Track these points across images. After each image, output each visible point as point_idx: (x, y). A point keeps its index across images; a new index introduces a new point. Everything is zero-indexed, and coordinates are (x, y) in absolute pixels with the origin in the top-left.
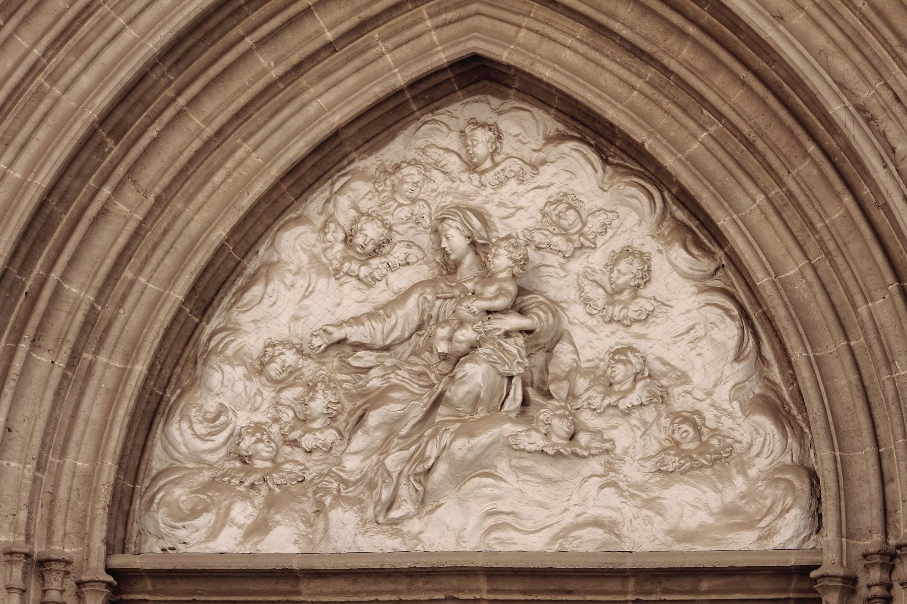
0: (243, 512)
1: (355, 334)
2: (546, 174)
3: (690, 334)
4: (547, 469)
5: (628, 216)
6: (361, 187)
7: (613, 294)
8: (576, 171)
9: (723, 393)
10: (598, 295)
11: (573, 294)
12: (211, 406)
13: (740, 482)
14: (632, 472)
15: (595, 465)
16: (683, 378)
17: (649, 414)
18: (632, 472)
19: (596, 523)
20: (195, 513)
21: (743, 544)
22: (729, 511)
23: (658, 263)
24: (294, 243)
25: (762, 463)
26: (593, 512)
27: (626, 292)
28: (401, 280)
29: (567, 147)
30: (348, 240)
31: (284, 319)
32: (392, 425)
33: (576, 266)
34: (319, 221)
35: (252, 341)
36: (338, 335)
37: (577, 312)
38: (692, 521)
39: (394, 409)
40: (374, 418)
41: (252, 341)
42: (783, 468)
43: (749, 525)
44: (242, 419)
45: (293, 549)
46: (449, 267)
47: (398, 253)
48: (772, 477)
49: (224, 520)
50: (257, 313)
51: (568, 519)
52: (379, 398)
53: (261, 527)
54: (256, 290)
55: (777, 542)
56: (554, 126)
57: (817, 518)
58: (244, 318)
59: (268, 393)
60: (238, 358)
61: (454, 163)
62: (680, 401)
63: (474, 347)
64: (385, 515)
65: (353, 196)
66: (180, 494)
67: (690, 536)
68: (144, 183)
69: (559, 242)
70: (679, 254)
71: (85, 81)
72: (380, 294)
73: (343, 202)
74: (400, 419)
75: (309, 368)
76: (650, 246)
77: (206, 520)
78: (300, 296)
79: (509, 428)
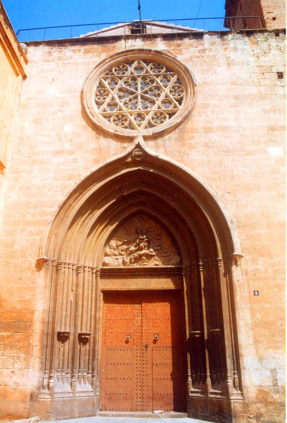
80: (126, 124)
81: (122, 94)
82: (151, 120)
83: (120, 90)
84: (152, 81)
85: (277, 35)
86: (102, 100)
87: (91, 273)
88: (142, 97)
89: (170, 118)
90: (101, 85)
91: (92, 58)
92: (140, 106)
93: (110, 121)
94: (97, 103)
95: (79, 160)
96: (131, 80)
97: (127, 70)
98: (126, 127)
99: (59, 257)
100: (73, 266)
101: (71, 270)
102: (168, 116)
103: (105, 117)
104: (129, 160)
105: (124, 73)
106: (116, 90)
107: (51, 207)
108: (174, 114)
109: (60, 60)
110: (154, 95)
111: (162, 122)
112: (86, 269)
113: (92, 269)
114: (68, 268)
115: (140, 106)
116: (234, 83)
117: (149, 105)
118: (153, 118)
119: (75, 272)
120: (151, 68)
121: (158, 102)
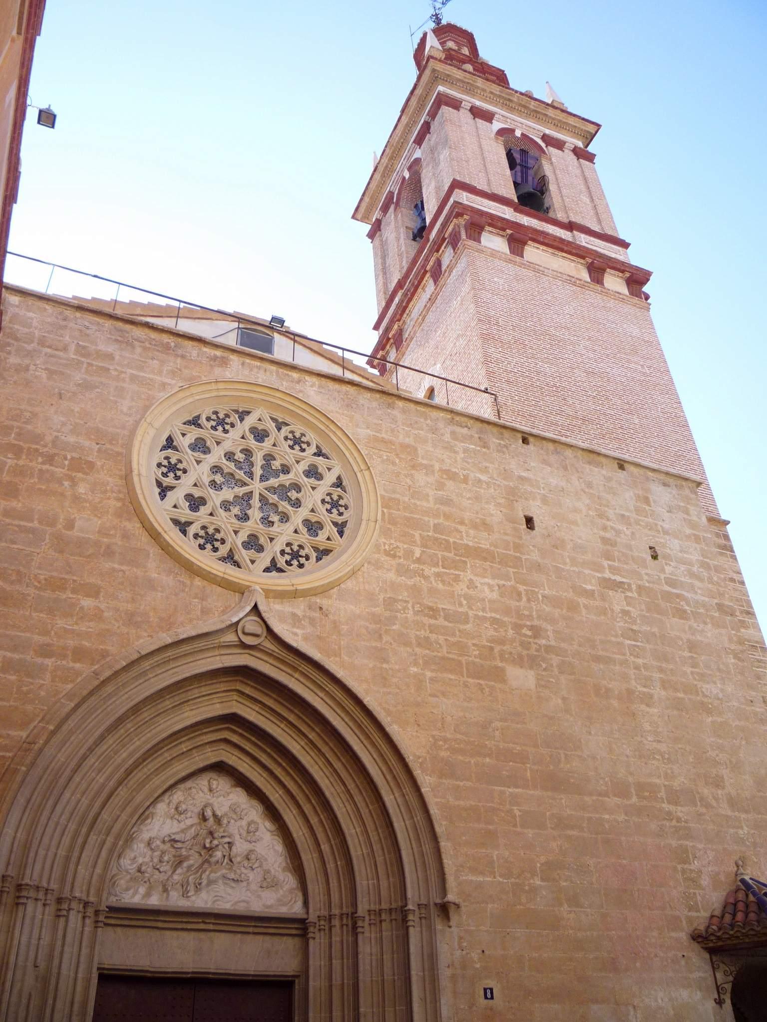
0: (142, 890)
1: (177, 837)
2: (231, 796)
3: (269, 847)
4: (233, 885)
5: (253, 812)
6: (180, 793)
7: (248, 832)
8: (239, 797)
9: (276, 865)
10: (244, 834)
11: (236, 832)
12: (132, 855)
13: (281, 891)
14: (253, 887)
15: (245, 884)
16: (266, 860)
17: (259, 869)
18: (253, 887)
19: (244, 901)
20: (128, 889)
21: (283, 911)
22: (279, 900)
23: (261, 827)
24: (161, 807)
25: (286, 887)
26: (243, 898)
27: (251, 831)
28: (189, 822)
29: (239, 789)
30: (177, 808)
31: (156, 831)
32: (189, 867)
33: (239, 823)
34: (167, 801)
35: (146, 836)
36: (173, 837)
37: (237, 837)
38: (269, 903)
39: (191, 862)
40: (185, 864)
41: (146, 836)
42: (294, 889)
43: (284, 905)
44: (140, 860)
45: (156, 903)
46: (204, 819)
47: (189, 815)
48: (291, 891)
49: (136, 892)
50: (149, 827)
51: (236, 899)
52: (187, 858)
53: (148, 895)
54: (149, 821)
55: (293, 911)
56: (233, 783)
57: (306, 903)
58: (145, 829)
59: (150, 853)
60: (142, 841)
61: (206, 790)
62: (265, 867)
63: (217, 846)
64: (185, 894)
65: (178, 796)
66: (122, 882)
67: (268, 907)
68: (129, 786)
69: (234, 816)
70: (268, 824)
71: (124, 755)
72: (182, 826)
73: (175, 797)
74: (192, 866)
75: (162, 847)
76: (259, 821)
77: (131, 892)
78: (162, 824)
79: (224, 871)
80: (223, 550)
81: (218, 478)
82: (279, 555)
83: (216, 469)
84: (286, 470)
85: (525, 441)
86: (169, 480)
87: (80, 915)
88: (262, 498)
89: (318, 559)
90: (170, 443)
91: (160, 373)
92: (255, 514)
93: (184, 532)
94: (159, 484)
95: (106, 614)
96: (241, 451)
97: (233, 425)
98: (223, 559)
99: (23, 866)
100: (46, 894)
101: (40, 904)
102: (314, 555)
103: (176, 522)
104: (231, 637)
105: (226, 431)
106: (205, 468)
107: (23, 725)
108: (327, 552)
109: (83, 356)
110: (289, 500)
111: (301, 566)
112: (74, 905)
113: (86, 904)
114: (36, 899)
115: (255, 514)
116: (447, 517)
117: (275, 518)
118: (283, 552)
119: (51, 909)
120: (286, 438)
121: (298, 517)
